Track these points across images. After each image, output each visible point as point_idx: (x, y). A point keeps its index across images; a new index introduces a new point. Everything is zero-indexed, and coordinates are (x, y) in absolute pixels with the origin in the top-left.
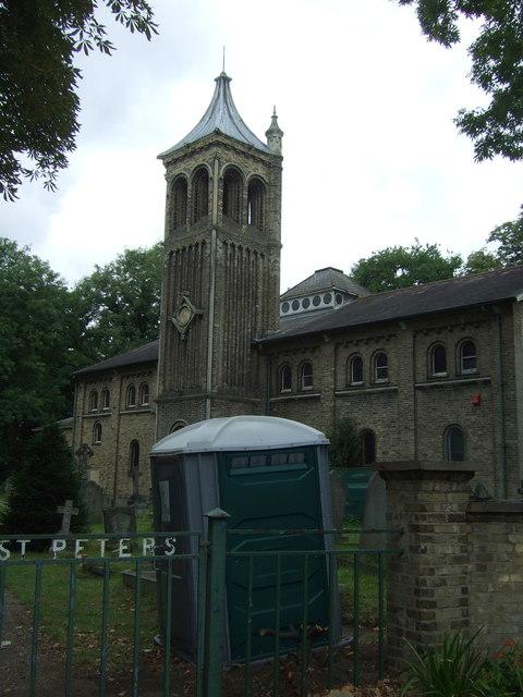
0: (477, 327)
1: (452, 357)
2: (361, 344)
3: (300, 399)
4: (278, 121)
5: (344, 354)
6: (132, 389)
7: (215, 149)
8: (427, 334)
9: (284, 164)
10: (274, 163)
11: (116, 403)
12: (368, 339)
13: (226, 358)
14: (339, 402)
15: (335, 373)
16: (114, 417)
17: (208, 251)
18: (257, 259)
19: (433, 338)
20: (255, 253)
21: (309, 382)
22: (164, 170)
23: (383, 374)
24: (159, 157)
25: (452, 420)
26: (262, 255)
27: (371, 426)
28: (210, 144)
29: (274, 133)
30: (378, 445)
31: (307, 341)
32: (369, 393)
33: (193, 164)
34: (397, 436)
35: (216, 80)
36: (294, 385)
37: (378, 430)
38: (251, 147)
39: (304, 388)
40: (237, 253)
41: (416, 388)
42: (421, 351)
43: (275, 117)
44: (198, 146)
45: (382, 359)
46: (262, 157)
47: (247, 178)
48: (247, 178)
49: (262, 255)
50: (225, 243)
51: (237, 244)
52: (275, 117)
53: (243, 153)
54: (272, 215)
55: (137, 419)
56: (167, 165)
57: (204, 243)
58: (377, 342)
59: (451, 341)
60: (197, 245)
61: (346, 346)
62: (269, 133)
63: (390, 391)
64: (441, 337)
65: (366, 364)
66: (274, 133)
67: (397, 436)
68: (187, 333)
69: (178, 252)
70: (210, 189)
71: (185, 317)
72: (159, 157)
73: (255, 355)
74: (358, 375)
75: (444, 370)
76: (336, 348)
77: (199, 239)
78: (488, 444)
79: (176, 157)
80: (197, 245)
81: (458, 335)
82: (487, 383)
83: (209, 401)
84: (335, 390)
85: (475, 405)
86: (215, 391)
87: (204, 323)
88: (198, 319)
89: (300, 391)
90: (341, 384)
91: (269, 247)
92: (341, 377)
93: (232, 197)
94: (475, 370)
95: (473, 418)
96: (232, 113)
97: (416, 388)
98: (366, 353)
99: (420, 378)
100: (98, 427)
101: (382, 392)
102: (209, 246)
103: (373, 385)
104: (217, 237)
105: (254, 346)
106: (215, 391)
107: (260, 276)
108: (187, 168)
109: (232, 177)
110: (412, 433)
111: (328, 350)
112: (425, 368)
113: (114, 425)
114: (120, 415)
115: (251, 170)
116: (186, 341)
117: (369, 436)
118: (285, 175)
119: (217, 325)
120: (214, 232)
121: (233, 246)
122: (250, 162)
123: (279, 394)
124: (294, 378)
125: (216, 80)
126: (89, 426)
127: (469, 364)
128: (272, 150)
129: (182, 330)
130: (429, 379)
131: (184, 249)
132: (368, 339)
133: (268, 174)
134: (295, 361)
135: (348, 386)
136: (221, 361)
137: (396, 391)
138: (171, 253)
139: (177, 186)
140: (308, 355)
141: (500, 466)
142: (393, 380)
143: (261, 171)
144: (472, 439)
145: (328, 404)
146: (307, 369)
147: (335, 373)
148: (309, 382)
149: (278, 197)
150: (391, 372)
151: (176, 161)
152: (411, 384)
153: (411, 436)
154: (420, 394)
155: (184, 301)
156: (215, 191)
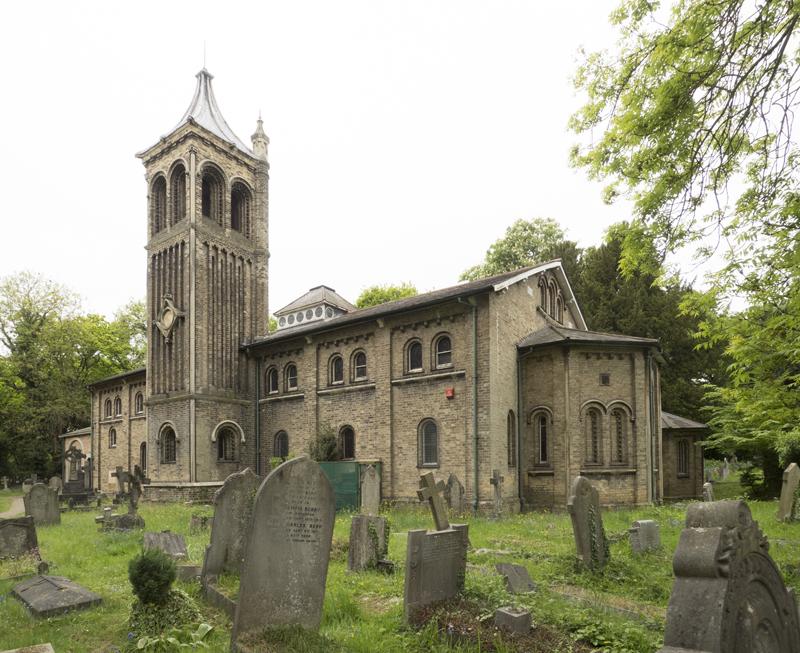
0: (453, 321)
1: (427, 355)
2: (341, 344)
3: (286, 399)
4: (264, 126)
5: (325, 355)
7: (190, 142)
8: (403, 332)
9: (270, 172)
10: (260, 169)
12: (348, 339)
13: (212, 359)
14: (322, 400)
15: (317, 373)
17: (187, 251)
18: (243, 265)
19: (409, 334)
20: (241, 259)
21: (294, 384)
22: (144, 170)
23: (362, 372)
24: (140, 156)
25: (426, 415)
26: (249, 261)
27: (351, 423)
29: (259, 137)
30: (357, 440)
31: (292, 343)
32: (349, 391)
34: (374, 431)
35: (197, 76)
36: (280, 386)
37: (357, 426)
38: (232, 147)
39: (291, 389)
40: (221, 257)
41: (393, 385)
42: (399, 346)
43: (260, 122)
45: (360, 358)
46: (247, 161)
47: (230, 181)
48: (230, 181)
49: (249, 261)
50: (206, 244)
51: (220, 248)
52: (260, 122)
53: (226, 153)
56: (147, 164)
57: (183, 244)
58: (357, 341)
59: (427, 337)
60: (177, 246)
61: (328, 348)
62: (254, 137)
63: (367, 389)
64: (418, 334)
65: (346, 363)
66: (259, 137)
67: (374, 431)
68: (170, 336)
69: (160, 255)
70: (187, 186)
71: (169, 320)
72: (140, 156)
73: (244, 360)
74: (339, 375)
75: (420, 366)
76: (318, 349)
77: (178, 240)
78: (461, 436)
79: (153, 154)
80: (177, 246)
81: (435, 330)
82: (461, 376)
83: (193, 402)
84: (317, 389)
85: (449, 398)
86: (200, 392)
87: (186, 324)
88: (180, 320)
89: (286, 392)
90: (323, 384)
91: (256, 255)
92: (323, 377)
93: (214, 198)
94: (449, 365)
95: (446, 411)
96: (214, 113)
97: (393, 385)
98: (346, 353)
99: (397, 374)
101: (361, 390)
102: (188, 245)
103: (352, 383)
104: (196, 236)
105: (242, 351)
106: (200, 392)
107: (248, 282)
108: (164, 166)
109: (211, 178)
110: (388, 428)
111: (311, 352)
112: (401, 365)
115: (233, 172)
116: (170, 344)
117: (348, 432)
118: (271, 183)
119: (199, 327)
120: (192, 231)
121: (215, 248)
122: (233, 163)
123: (267, 395)
124: (281, 379)
125: (197, 76)
127: (444, 358)
128: (257, 156)
129: (166, 333)
130: (406, 375)
131: (165, 252)
132: (348, 339)
133: (254, 180)
134: (281, 364)
135: (330, 385)
136: (205, 363)
137: (373, 388)
138: (154, 257)
139: (158, 184)
140: (293, 358)
141: (472, 456)
142: (371, 377)
143: (246, 176)
144: (445, 431)
145: (310, 403)
146: (292, 370)
147: (317, 373)
148: (294, 384)
149: (265, 204)
150: (369, 370)
151: (154, 159)
152: (388, 381)
153: (387, 431)
154: (395, 389)
156: (193, 188)
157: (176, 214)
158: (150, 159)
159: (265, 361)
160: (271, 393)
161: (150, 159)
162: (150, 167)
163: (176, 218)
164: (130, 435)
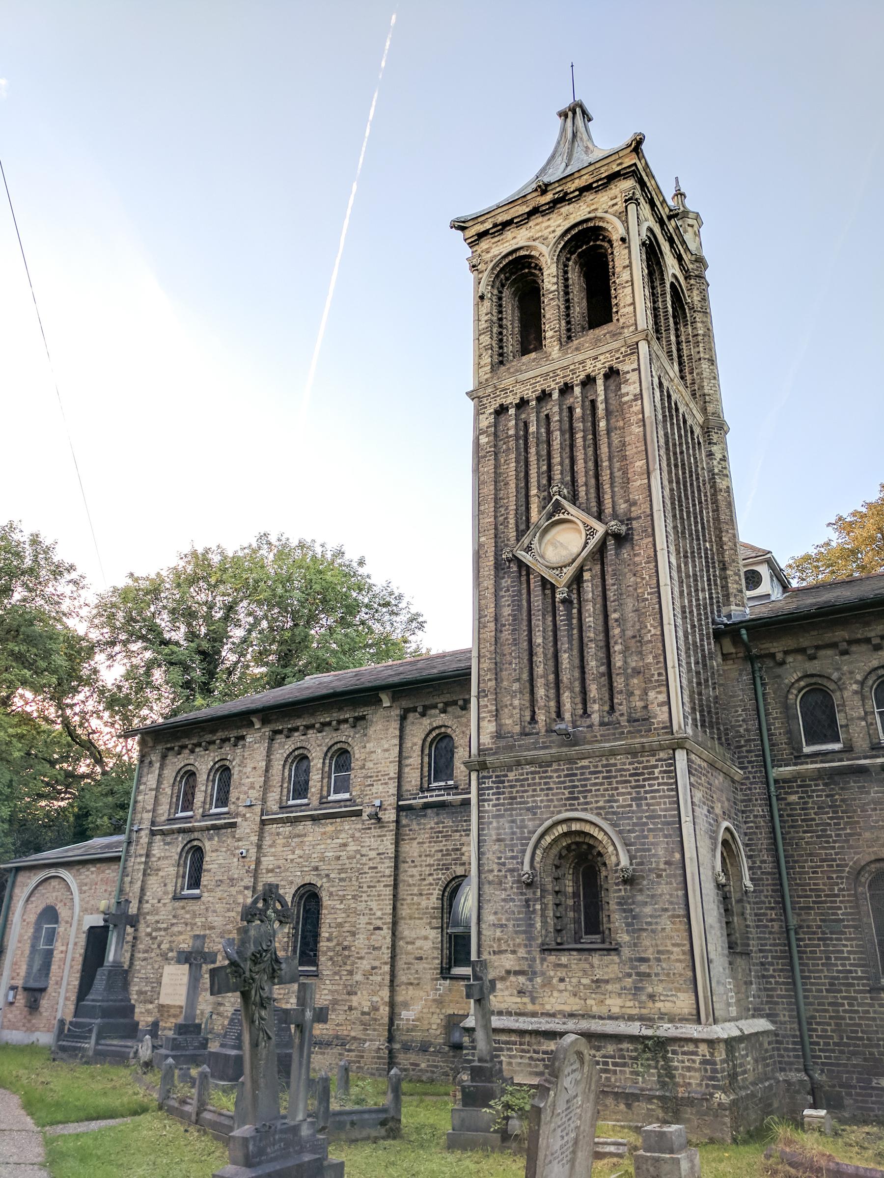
6: (301, 759)
11: (254, 794)
16: (247, 827)
24: (460, 226)
28: (613, 177)
33: (557, 224)
35: (564, 115)
44: (571, 187)
54: (705, 365)
55: (313, 833)
72: (460, 226)
77: (597, 368)
79: (501, 219)
80: (589, 381)
100: (196, 857)
113: (248, 845)
114: (263, 823)
125: (564, 115)
126: (167, 856)
138: (501, 410)
155: (558, 508)
157: (568, 323)
158: (477, 230)
159: (783, 663)
160: (807, 750)
161: (477, 230)
162: (484, 244)
163: (569, 330)
164: (258, 862)
